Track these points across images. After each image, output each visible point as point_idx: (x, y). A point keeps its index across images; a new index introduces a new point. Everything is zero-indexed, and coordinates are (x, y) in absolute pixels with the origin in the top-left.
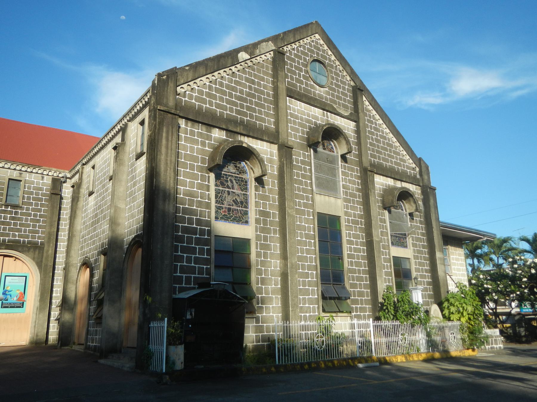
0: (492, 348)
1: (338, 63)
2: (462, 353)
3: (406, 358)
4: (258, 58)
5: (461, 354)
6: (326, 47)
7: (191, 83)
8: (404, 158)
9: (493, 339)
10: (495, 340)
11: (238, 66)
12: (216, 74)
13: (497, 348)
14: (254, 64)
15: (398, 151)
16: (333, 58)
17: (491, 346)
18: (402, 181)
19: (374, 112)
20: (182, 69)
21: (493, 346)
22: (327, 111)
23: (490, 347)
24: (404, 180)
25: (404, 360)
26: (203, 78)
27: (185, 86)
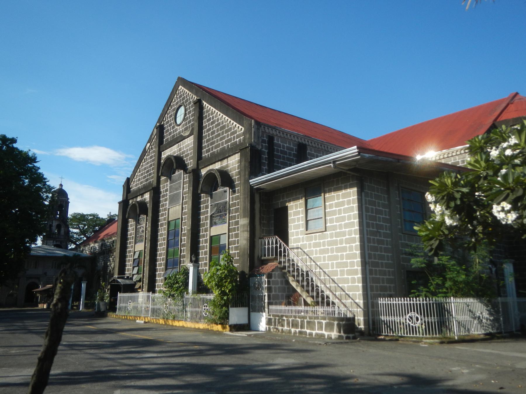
0: (300, 332)
1: (190, 93)
2: (211, 327)
3: (165, 322)
4: (154, 140)
5: (209, 327)
6: (184, 89)
7: (134, 180)
8: (235, 129)
9: (305, 320)
10: (308, 322)
11: (147, 154)
12: (140, 167)
13: (311, 334)
14: (153, 145)
15: (230, 127)
16: (188, 92)
17: (299, 329)
18: (227, 157)
19: (212, 108)
20: (132, 175)
21: (303, 330)
22: (180, 142)
23: (297, 330)
24: (227, 156)
25: (164, 323)
26: (137, 174)
27: (132, 183)
